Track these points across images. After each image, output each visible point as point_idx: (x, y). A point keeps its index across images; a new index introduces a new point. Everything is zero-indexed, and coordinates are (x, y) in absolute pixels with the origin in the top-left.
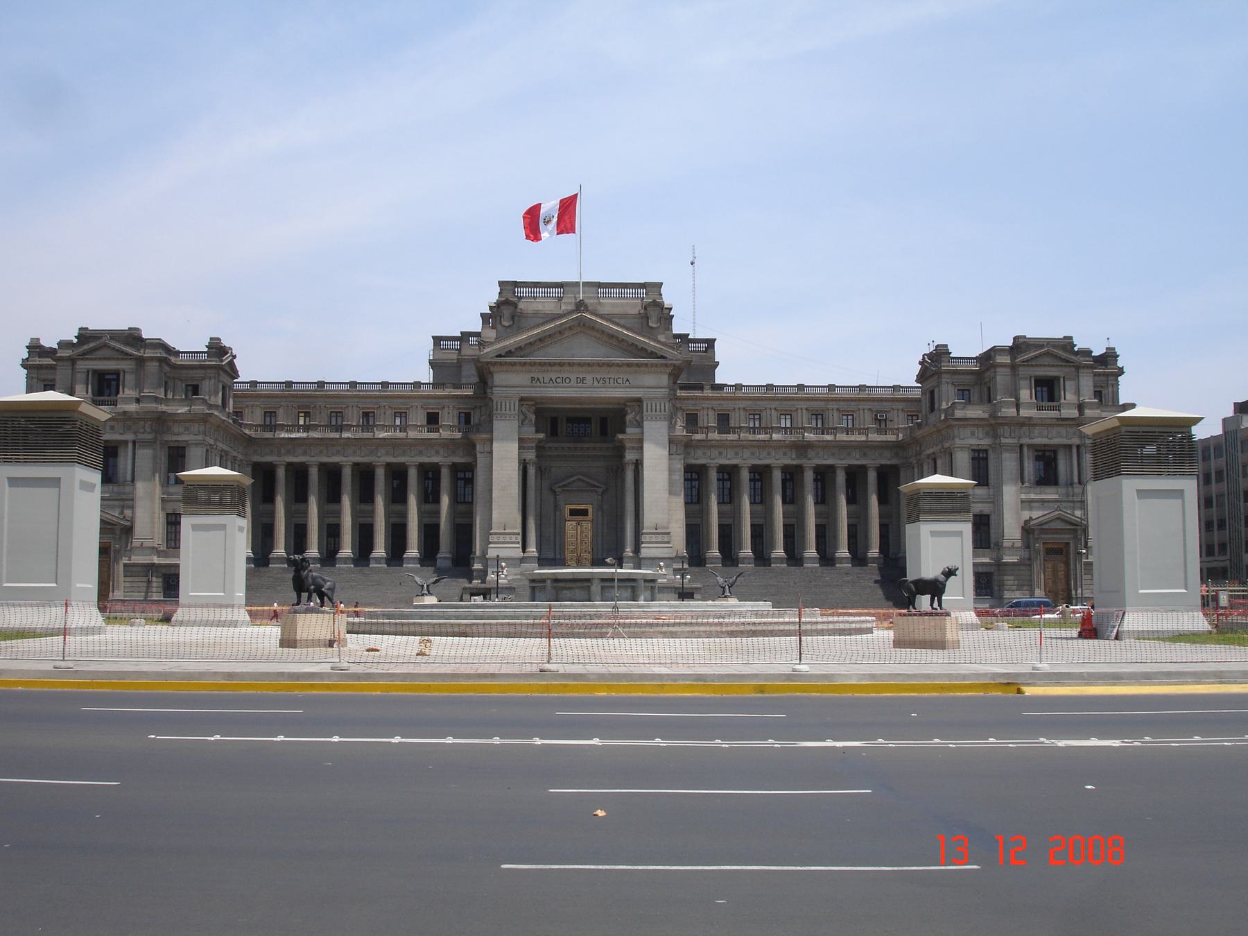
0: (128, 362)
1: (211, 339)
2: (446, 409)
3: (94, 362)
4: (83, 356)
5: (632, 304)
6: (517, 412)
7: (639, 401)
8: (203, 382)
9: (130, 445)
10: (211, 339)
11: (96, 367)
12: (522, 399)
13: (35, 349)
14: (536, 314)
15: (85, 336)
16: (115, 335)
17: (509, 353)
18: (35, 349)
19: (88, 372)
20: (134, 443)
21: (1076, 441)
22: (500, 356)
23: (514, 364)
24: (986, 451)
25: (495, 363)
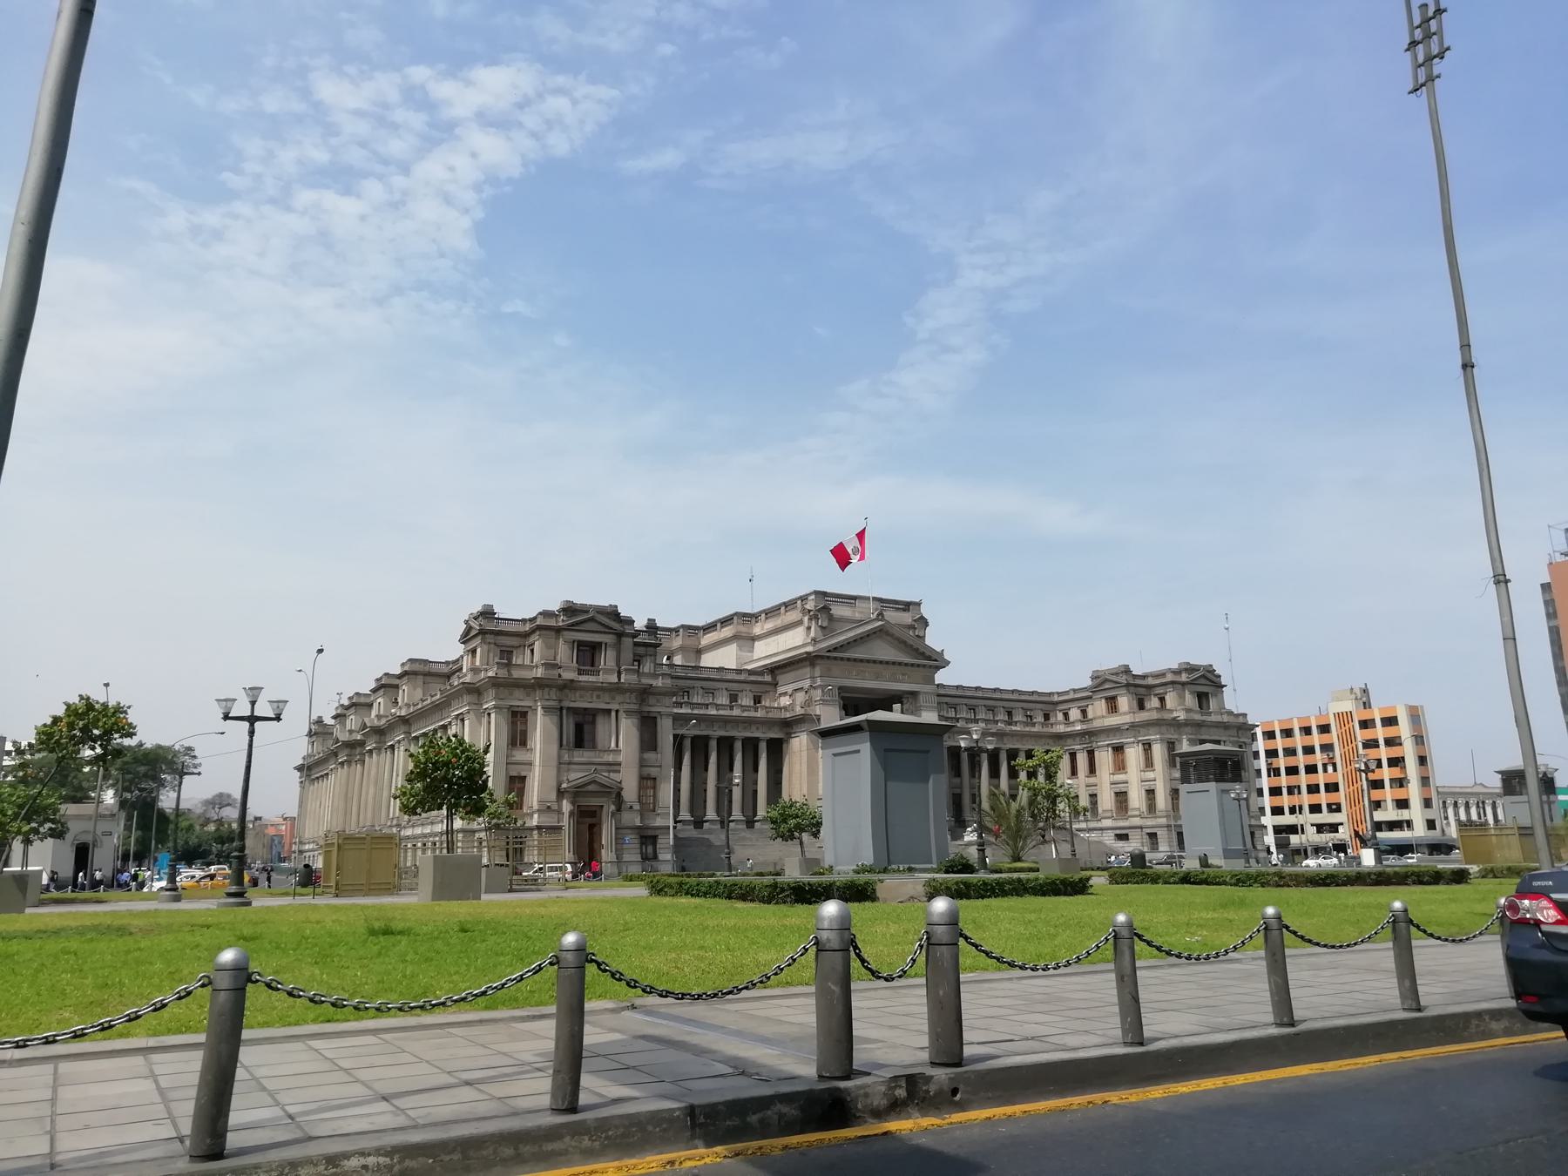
0: (611, 636)
1: (649, 620)
2: (744, 692)
3: (579, 634)
4: (571, 628)
5: (907, 618)
6: (837, 698)
7: (914, 694)
8: (644, 659)
9: (613, 714)
10: (649, 620)
11: (581, 638)
12: (840, 688)
13: (487, 613)
14: (842, 620)
15: (570, 609)
16: (601, 610)
17: (835, 649)
18: (487, 613)
19: (574, 642)
20: (617, 711)
21: (1224, 739)
22: (829, 651)
23: (835, 658)
24: (1173, 743)
25: (822, 657)
